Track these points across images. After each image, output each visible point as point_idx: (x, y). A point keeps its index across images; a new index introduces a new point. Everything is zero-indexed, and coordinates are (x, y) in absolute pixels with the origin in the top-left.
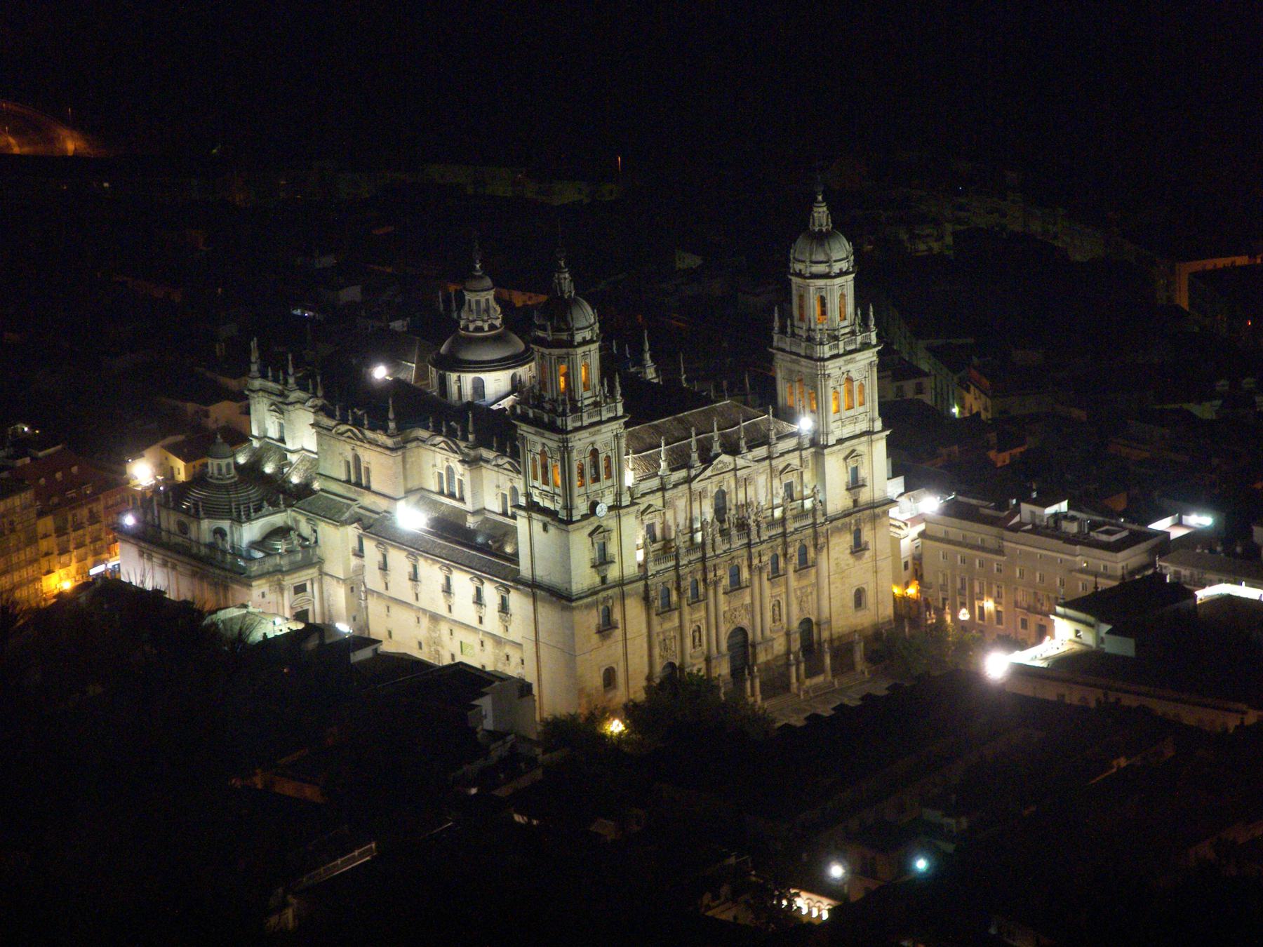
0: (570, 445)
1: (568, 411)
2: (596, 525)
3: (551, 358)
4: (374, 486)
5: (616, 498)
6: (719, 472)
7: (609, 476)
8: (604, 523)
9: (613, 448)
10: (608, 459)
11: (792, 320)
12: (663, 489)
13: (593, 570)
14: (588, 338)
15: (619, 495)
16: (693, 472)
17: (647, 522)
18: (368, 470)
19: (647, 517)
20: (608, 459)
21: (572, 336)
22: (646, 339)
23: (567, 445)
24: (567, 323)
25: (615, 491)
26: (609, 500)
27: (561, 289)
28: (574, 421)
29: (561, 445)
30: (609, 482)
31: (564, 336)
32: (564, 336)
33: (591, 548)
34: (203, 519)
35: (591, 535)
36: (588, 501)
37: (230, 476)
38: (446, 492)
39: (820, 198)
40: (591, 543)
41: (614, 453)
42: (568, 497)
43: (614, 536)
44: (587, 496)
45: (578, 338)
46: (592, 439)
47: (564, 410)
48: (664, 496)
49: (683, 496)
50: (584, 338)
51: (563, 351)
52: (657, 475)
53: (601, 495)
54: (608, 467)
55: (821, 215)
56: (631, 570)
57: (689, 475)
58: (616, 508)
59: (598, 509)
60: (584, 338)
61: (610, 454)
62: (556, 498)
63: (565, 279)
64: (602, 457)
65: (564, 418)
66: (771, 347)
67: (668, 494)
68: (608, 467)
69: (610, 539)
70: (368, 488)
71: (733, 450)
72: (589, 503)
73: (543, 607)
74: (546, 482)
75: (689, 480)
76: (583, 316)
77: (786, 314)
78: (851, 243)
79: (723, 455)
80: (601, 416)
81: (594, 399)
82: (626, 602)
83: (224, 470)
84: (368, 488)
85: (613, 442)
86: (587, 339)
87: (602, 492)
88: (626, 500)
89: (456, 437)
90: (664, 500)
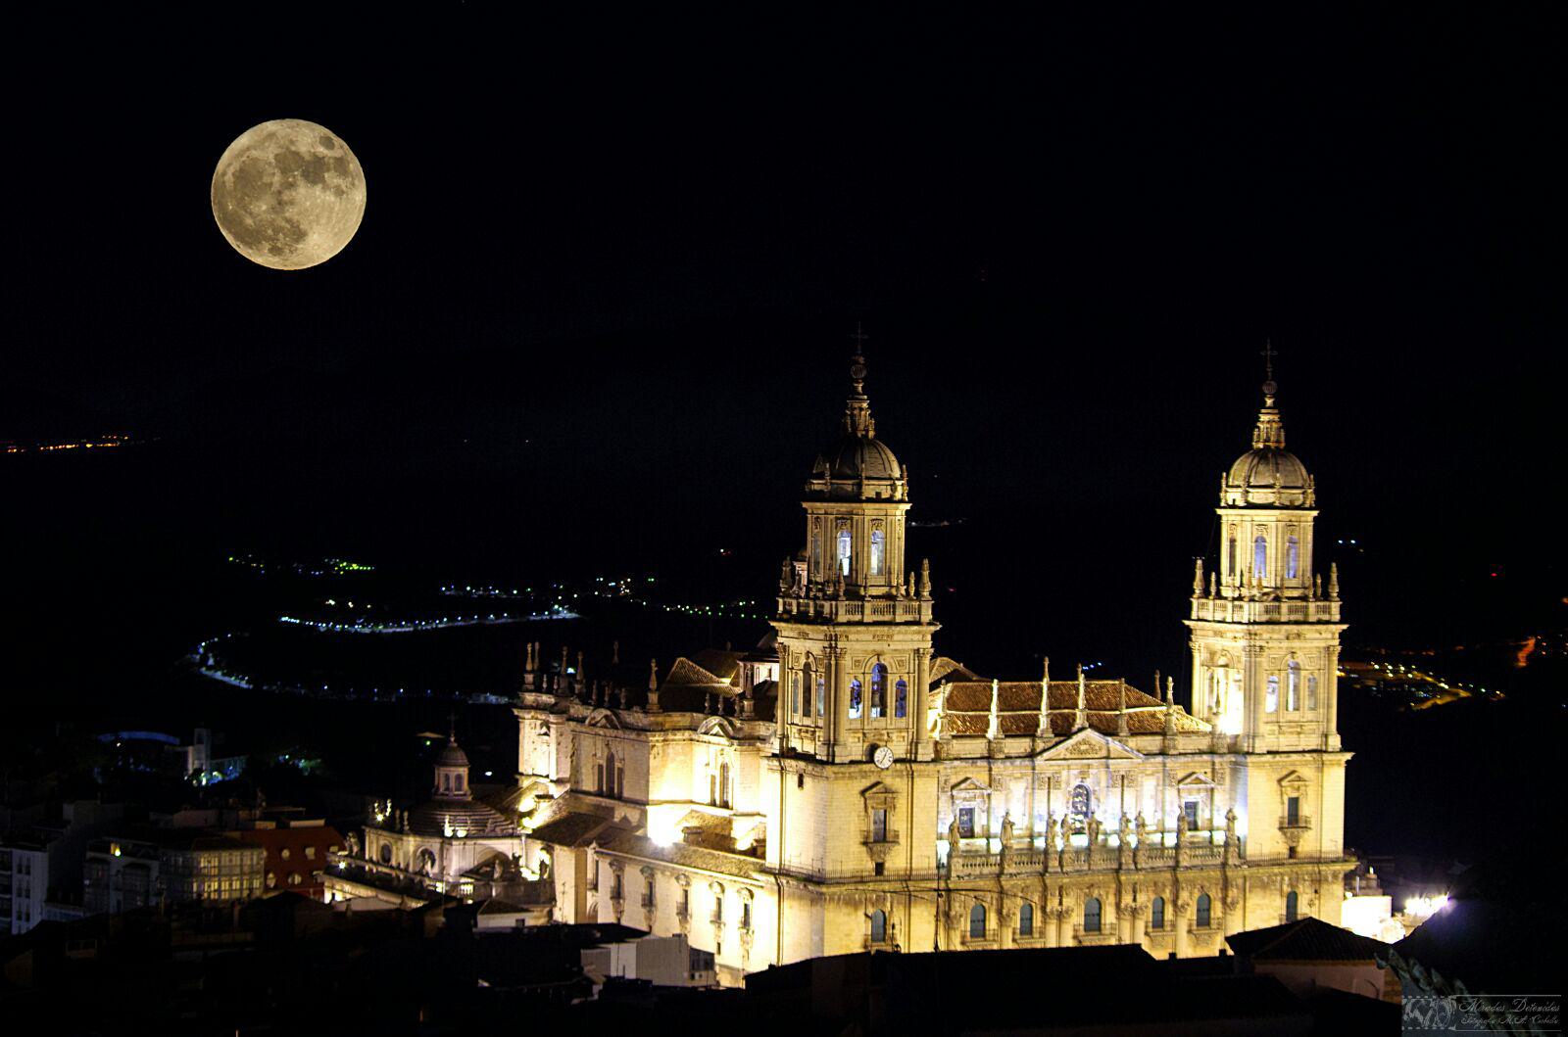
0: (840, 645)
1: (841, 594)
2: (873, 780)
3: (826, 520)
4: (626, 794)
5: (911, 749)
6: (1080, 756)
7: (901, 711)
8: (888, 781)
9: (912, 671)
10: (901, 685)
11: (1219, 575)
12: (989, 758)
13: (864, 849)
14: (885, 496)
15: (915, 744)
16: (1040, 745)
17: (960, 804)
18: (621, 771)
19: (963, 794)
20: (901, 685)
21: (860, 485)
22: (1046, 670)
23: (836, 644)
24: (855, 467)
25: (910, 737)
26: (900, 749)
27: (853, 422)
28: (848, 612)
29: (826, 644)
30: (902, 722)
31: (848, 485)
32: (848, 485)
33: (863, 813)
34: (408, 835)
35: (863, 793)
36: (864, 741)
37: (462, 793)
38: (718, 802)
39: (1269, 402)
40: (863, 806)
41: (912, 679)
42: (832, 727)
43: (902, 803)
44: (864, 734)
45: (869, 491)
46: (878, 646)
47: (837, 591)
48: (990, 770)
49: (1021, 778)
50: (878, 494)
51: (844, 507)
52: (984, 737)
53: (886, 737)
54: (902, 698)
55: (1267, 423)
56: (924, 862)
57: (1033, 750)
58: (908, 761)
59: (878, 755)
60: (878, 494)
61: (905, 678)
62: (817, 734)
63: (861, 409)
64: (892, 680)
65: (834, 603)
66: (1189, 619)
67: (997, 767)
68: (902, 698)
69: (895, 808)
70: (620, 798)
71: (1108, 729)
72: (866, 745)
73: (791, 907)
74: (807, 713)
75: (1032, 755)
76: (881, 462)
77: (1213, 565)
78: (1312, 476)
79: (1089, 730)
80: (894, 614)
81: (886, 589)
82: (912, 910)
83: (452, 783)
84: (620, 798)
85: (912, 662)
86: (883, 497)
87: (888, 733)
88: (926, 752)
89: (733, 716)
90: (990, 775)
